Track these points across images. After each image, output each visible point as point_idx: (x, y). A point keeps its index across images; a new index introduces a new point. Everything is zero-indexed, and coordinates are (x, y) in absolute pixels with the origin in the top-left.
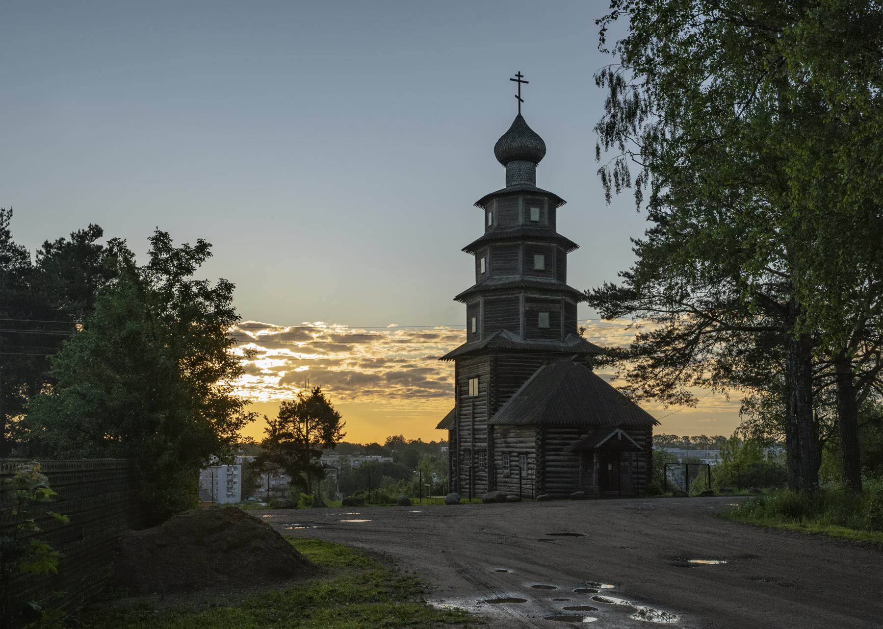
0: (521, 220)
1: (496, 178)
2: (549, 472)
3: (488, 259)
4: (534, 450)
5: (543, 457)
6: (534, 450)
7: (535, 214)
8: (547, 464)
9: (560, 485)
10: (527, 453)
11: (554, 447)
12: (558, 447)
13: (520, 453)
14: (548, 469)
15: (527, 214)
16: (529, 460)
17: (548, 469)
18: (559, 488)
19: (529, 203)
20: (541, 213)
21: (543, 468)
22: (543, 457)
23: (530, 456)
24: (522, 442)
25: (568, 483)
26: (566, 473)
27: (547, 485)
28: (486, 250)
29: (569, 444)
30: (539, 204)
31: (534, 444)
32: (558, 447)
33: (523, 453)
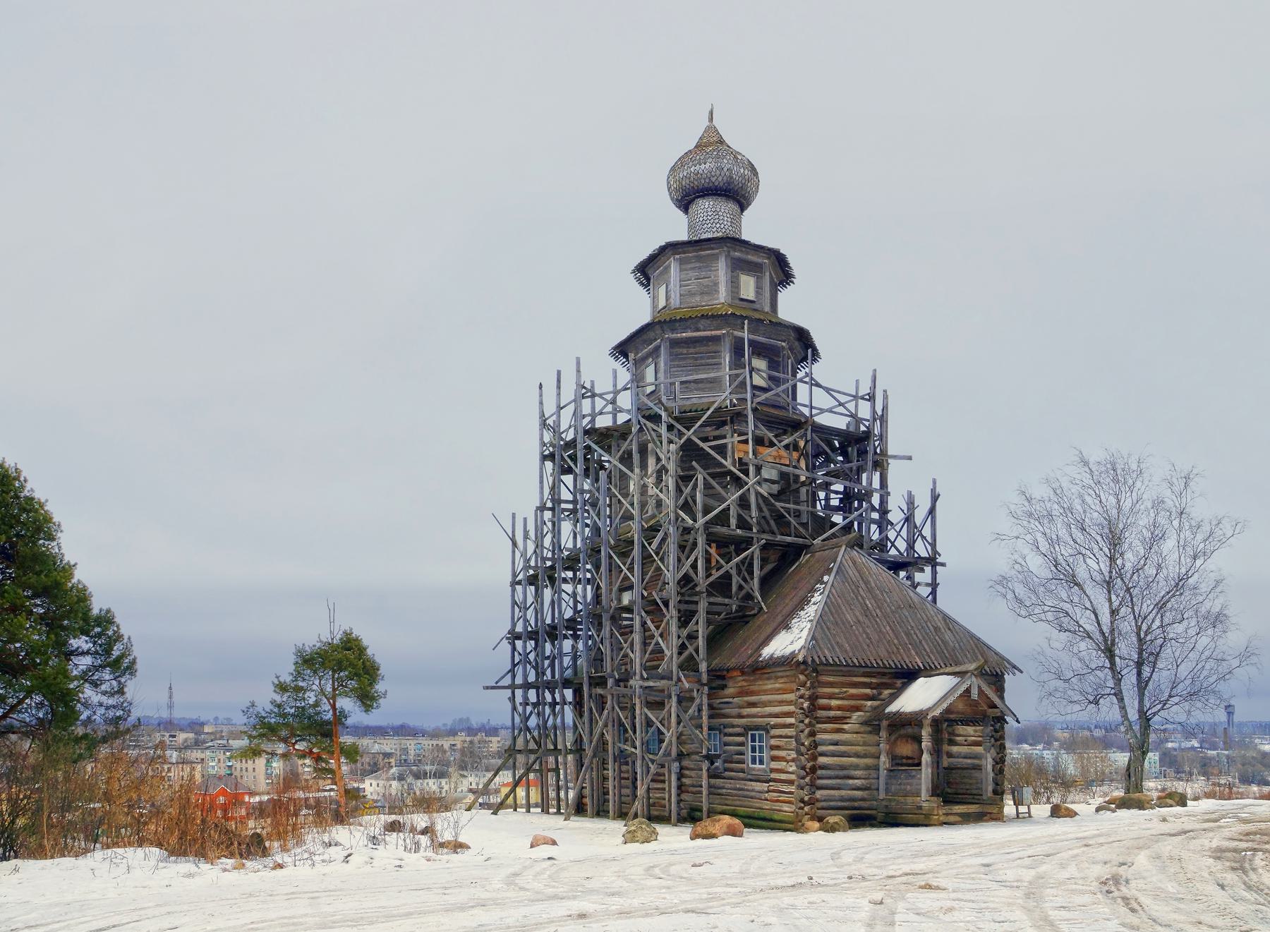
0: (723, 295)
2: (823, 767)
3: (662, 364)
4: (792, 720)
6: (792, 720)
8: (821, 749)
9: (843, 793)
10: (766, 729)
11: (832, 713)
12: (839, 713)
13: (747, 728)
14: (822, 760)
15: (734, 285)
16: (773, 742)
17: (822, 760)
18: (842, 799)
19: (739, 266)
20: (759, 288)
21: (814, 758)
22: (812, 734)
23: (773, 732)
24: (753, 705)
25: (858, 789)
26: (856, 767)
27: (819, 794)
28: (657, 349)
29: (857, 709)
30: (754, 269)
31: (792, 708)
32: (839, 713)
33: (757, 728)
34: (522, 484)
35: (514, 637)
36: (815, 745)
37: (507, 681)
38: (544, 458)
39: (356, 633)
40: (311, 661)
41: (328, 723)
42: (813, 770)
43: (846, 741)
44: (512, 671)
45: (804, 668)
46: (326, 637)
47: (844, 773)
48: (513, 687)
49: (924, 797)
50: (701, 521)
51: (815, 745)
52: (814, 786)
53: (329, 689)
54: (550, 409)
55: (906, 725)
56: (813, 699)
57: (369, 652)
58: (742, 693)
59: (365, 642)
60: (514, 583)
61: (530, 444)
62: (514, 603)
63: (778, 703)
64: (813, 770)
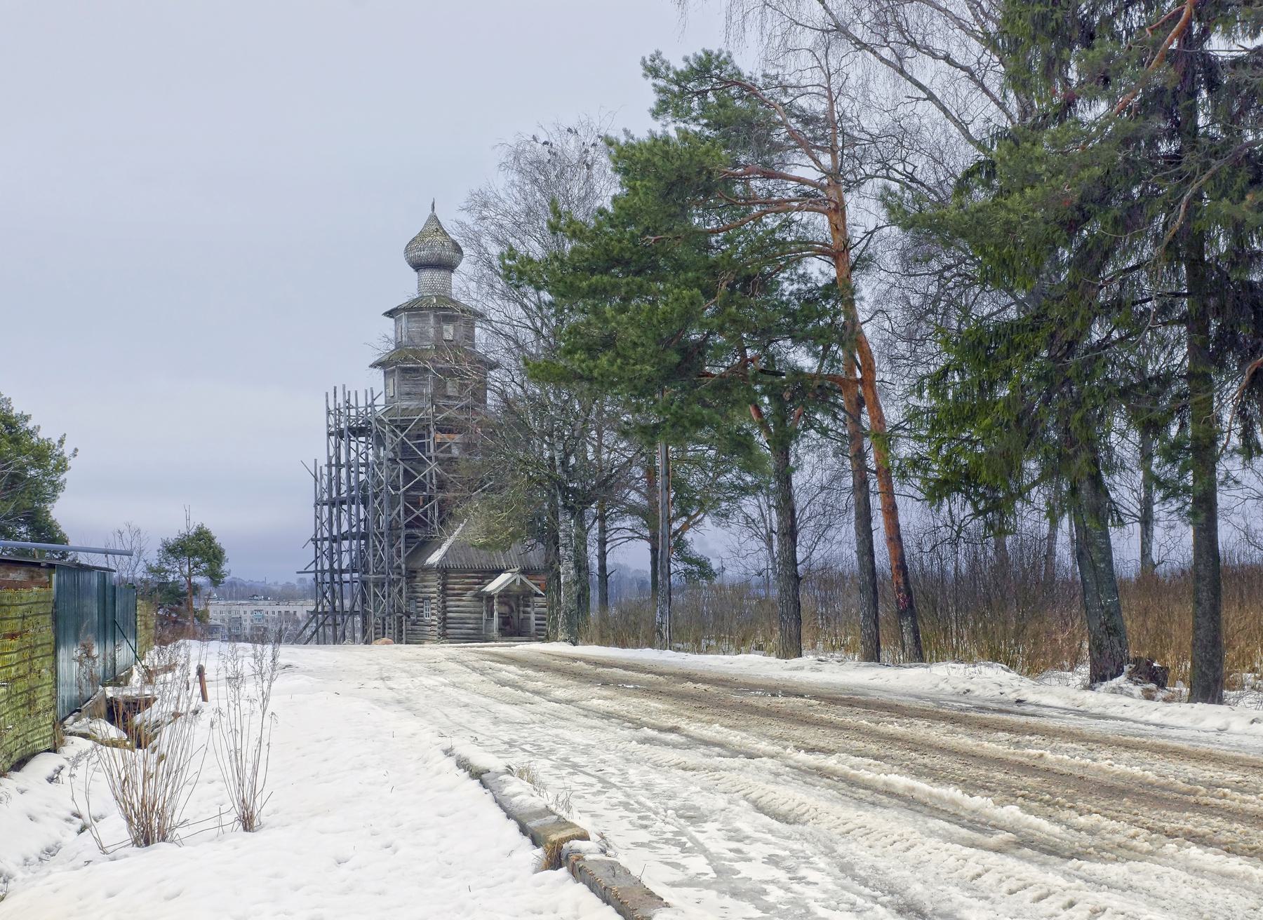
1: (407, 285)
5: (444, 602)
7: (449, 332)
13: (424, 599)
14: (450, 615)
15: (439, 332)
17: (450, 615)
21: (444, 613)
22: (444, 602)
34: (318, 449)
35: (315, 540)
36: (445, 607)
37: (312, 568)
38: (330, 434)
39: (206, 526)
40: (177, 550)
41: (185, 594)
42: (444, 619)
43: (462, 606)
44: (315, 561)
45: (443, 571)
46: (184, 531)
47: (462, 621)
48: (316, 572)
49: (495, 633)
50: (402, 490)
51: (445, 607)
52: (445, 627)
53: (186, 569)
54: (332, 408)
55: (490, 597)
56: (444, 585)
57: (216, 541)
58: (423, 581)
59: (213, 534)
60: (317, 504)
61: (320, 424)
62: (317, 517)
63: (432, 586)
64: (444, 619)
